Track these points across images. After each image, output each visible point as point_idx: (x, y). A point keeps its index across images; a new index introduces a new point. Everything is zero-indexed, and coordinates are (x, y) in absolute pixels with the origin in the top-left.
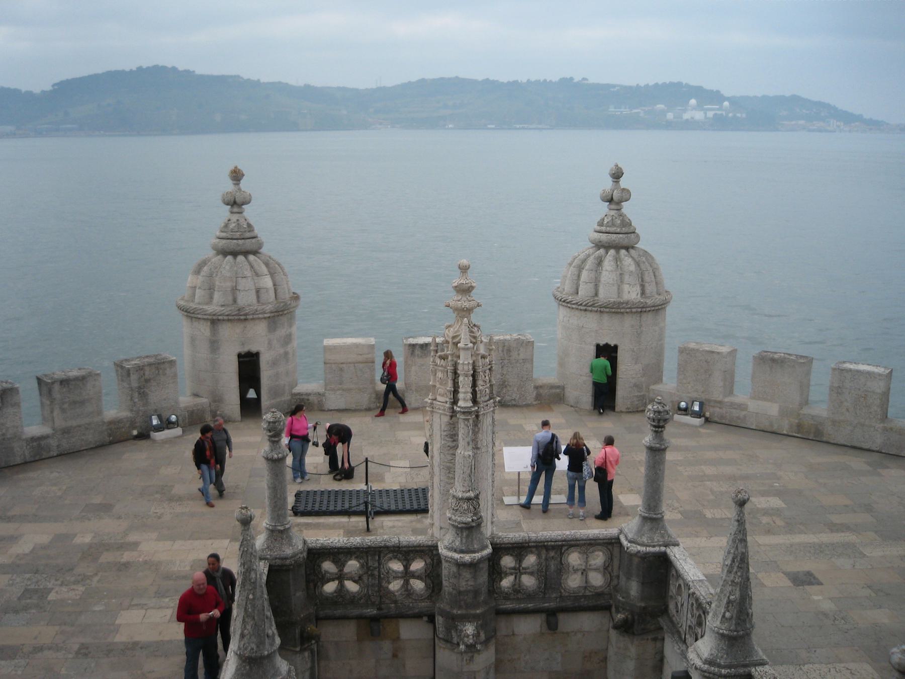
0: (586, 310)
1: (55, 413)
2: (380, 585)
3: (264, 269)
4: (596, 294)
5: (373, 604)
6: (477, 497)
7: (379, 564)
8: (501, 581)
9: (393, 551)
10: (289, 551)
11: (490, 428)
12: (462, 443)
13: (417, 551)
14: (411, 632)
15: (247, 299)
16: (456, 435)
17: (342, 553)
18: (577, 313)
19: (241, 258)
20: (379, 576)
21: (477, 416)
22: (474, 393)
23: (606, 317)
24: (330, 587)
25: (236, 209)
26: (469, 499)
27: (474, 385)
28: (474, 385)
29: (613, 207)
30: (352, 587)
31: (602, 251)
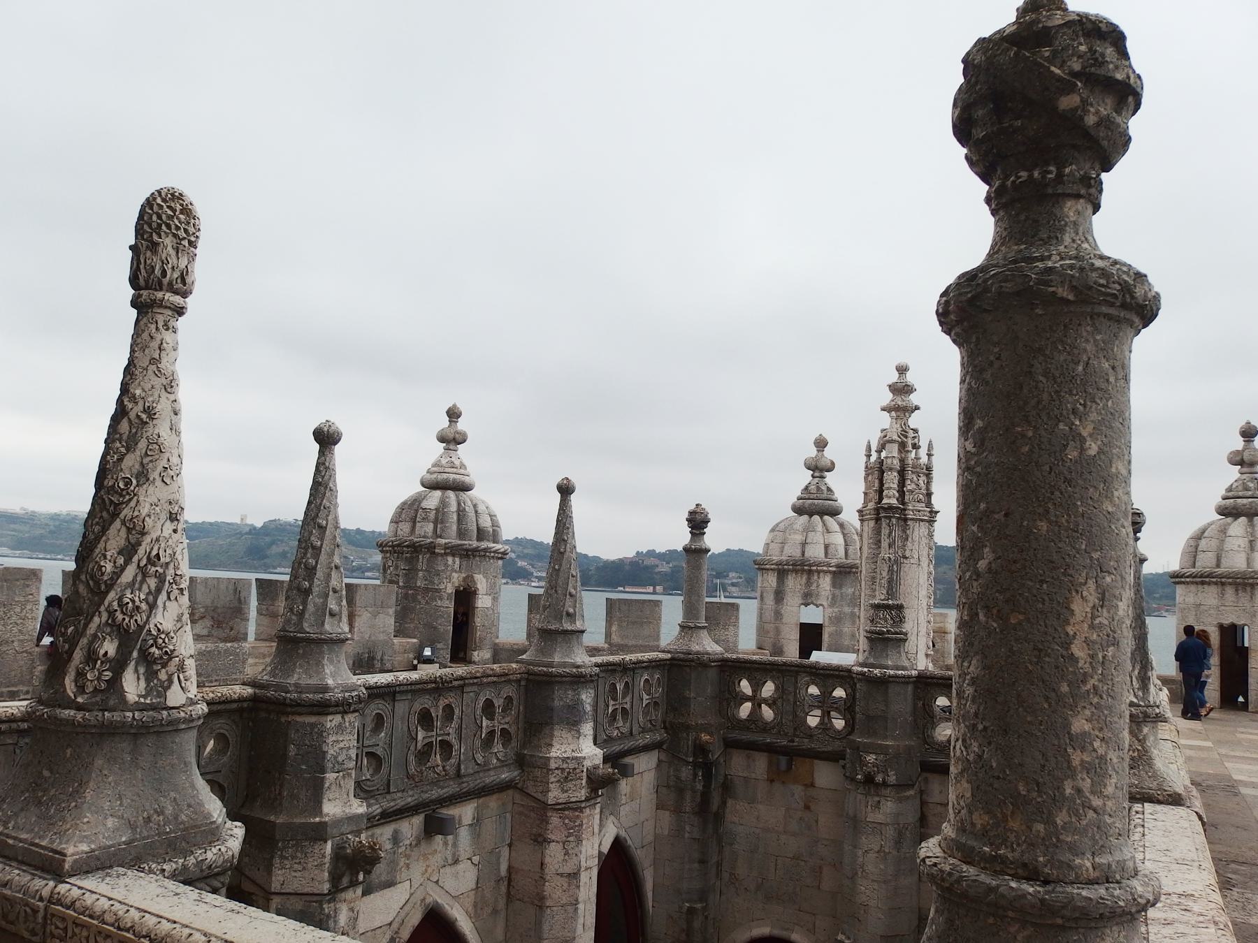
0: (1203, 583)
1: (614, 628)
2: (795, 715)
3: (837, 528)
4: (1218, 566)
5: (786, 734)
6: (900, 608)
7: (796, 688)
8: (934, 728)
9: (811, 674)
10: (695, 648)
11: (924, 541)
12: (885, 544)
13: (838, 677)
14: (826, 775)
15: (815, 552)
16: (880, 541)
17: (757, 670)
18: (1193, 588)
19: (816, 518)
20: (795, 703)
21: (906, 520)
22: (902, 493)
23: (1230, 591)
24: (745, 710)
25: (817, 474)
26: (887, 607)
27: (902, 483)
28: (902, 483)
29: (1245, 470)
30: (767, 713)
31: (1229, 520)
